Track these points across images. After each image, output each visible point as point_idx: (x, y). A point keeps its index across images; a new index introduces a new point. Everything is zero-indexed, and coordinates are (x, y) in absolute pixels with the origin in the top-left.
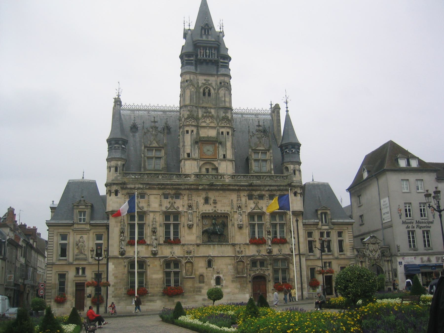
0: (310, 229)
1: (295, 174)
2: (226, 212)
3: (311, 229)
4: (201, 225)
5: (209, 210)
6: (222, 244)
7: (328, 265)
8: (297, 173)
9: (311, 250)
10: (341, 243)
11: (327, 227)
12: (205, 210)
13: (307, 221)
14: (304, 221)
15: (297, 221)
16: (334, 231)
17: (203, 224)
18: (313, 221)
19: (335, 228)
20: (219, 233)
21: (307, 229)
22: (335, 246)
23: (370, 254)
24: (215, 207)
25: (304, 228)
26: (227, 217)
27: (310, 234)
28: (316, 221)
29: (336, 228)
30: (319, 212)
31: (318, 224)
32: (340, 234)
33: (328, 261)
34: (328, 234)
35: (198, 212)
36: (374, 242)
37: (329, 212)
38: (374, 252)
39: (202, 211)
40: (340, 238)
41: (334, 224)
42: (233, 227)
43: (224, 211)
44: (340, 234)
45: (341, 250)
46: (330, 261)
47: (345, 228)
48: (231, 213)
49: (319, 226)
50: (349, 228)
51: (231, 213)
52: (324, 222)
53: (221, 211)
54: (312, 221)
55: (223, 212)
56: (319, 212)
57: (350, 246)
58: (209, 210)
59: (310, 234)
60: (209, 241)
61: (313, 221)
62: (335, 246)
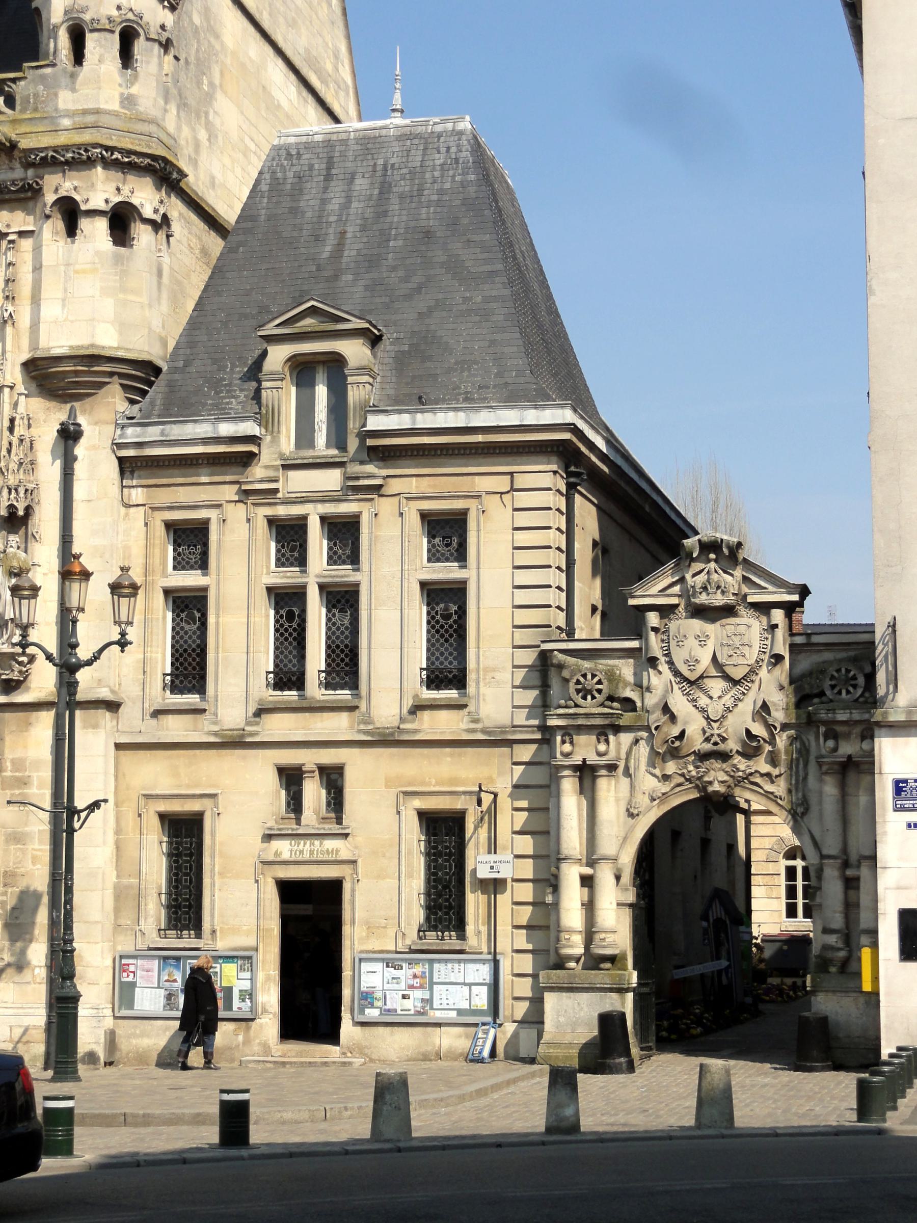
0: (184, 495)
1: (78, 56)
3: (193, 496)
7: (314, 793)
8: (101, 50)
9: (190, 669)
10: (447, 607)
11: (331, 480)
13: (153, 433)
14: (132, 434)
15: (69, 435)
16: (386, 506)
18: (203, 429)
19: (395, 486)
21: (165, 496)
22: (395, 640)
23: (679, 703)
25: (137, 495)
27: (190, 540)
28: (226, 429)
29: (413, 486)
30: (278, 356)
31: (247, 459)
32: (447, 532)
33: (308, 759)
34: (344, 534)
36: (718, 600)
37: (354, 351)
38: (716, 686)
40: (448, 571)
41: (385, 453)
44: (447, 532)
45: (448, 670)
46: (328, 757)
47: (484, 484)
49: (258, 471)
50: (522, 481)
52: (321, 439)
54: (195, 433)
56: (278, 356)
57: (523, 637)
59: (190, 540)
61: (203, 429)
62: (395, 640)
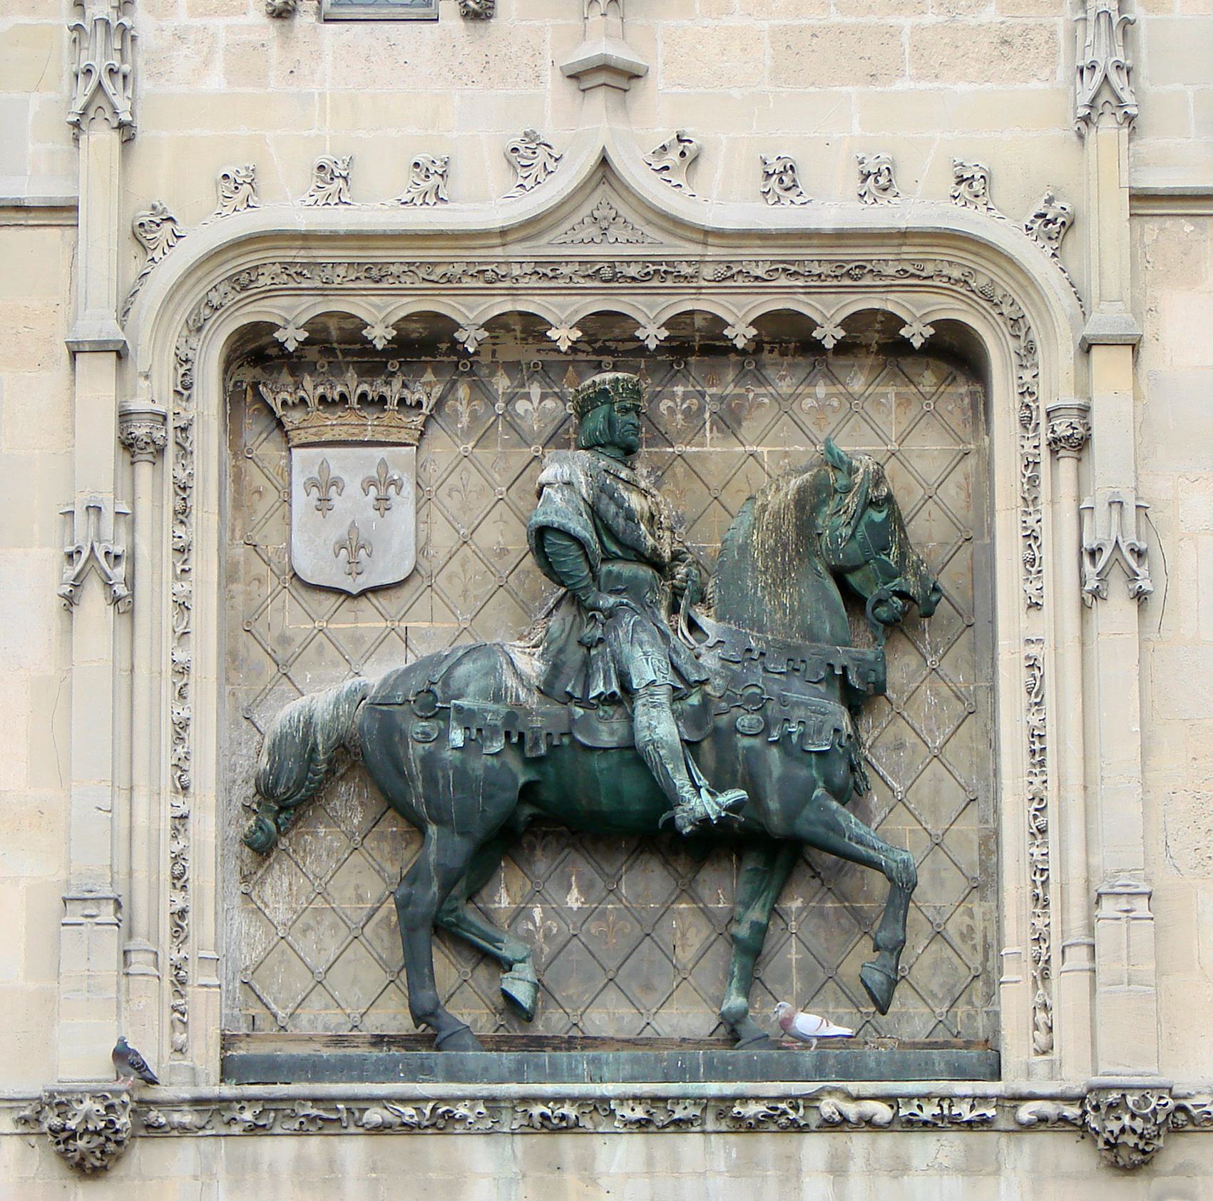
2: (921, 205)
4: (187, 595)
5: (433, 176)
6: (784, 1121)
12: (331, 176)
17: (253, 564)
20: (701, 803)
24: (613, 77)
26: (956, 353)
35: (100, 226)
39: (239, 186)
42: (1117, 609)
43: (878, 180)
48: (1057, 227)
51: (1057, 227)
53: (783, 178)
55: (833, 206)
58: (433, 176)
60: (430, 1033)
